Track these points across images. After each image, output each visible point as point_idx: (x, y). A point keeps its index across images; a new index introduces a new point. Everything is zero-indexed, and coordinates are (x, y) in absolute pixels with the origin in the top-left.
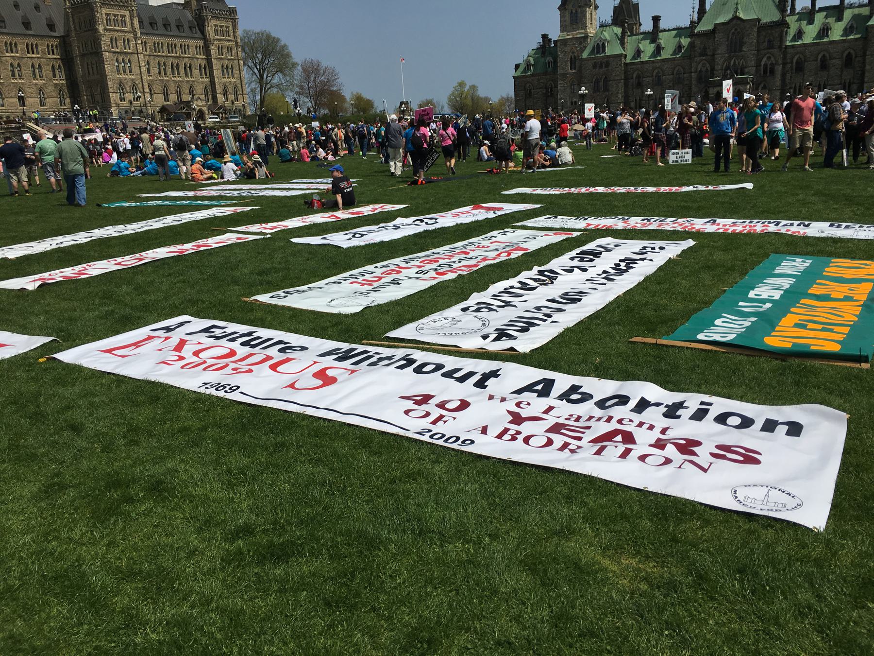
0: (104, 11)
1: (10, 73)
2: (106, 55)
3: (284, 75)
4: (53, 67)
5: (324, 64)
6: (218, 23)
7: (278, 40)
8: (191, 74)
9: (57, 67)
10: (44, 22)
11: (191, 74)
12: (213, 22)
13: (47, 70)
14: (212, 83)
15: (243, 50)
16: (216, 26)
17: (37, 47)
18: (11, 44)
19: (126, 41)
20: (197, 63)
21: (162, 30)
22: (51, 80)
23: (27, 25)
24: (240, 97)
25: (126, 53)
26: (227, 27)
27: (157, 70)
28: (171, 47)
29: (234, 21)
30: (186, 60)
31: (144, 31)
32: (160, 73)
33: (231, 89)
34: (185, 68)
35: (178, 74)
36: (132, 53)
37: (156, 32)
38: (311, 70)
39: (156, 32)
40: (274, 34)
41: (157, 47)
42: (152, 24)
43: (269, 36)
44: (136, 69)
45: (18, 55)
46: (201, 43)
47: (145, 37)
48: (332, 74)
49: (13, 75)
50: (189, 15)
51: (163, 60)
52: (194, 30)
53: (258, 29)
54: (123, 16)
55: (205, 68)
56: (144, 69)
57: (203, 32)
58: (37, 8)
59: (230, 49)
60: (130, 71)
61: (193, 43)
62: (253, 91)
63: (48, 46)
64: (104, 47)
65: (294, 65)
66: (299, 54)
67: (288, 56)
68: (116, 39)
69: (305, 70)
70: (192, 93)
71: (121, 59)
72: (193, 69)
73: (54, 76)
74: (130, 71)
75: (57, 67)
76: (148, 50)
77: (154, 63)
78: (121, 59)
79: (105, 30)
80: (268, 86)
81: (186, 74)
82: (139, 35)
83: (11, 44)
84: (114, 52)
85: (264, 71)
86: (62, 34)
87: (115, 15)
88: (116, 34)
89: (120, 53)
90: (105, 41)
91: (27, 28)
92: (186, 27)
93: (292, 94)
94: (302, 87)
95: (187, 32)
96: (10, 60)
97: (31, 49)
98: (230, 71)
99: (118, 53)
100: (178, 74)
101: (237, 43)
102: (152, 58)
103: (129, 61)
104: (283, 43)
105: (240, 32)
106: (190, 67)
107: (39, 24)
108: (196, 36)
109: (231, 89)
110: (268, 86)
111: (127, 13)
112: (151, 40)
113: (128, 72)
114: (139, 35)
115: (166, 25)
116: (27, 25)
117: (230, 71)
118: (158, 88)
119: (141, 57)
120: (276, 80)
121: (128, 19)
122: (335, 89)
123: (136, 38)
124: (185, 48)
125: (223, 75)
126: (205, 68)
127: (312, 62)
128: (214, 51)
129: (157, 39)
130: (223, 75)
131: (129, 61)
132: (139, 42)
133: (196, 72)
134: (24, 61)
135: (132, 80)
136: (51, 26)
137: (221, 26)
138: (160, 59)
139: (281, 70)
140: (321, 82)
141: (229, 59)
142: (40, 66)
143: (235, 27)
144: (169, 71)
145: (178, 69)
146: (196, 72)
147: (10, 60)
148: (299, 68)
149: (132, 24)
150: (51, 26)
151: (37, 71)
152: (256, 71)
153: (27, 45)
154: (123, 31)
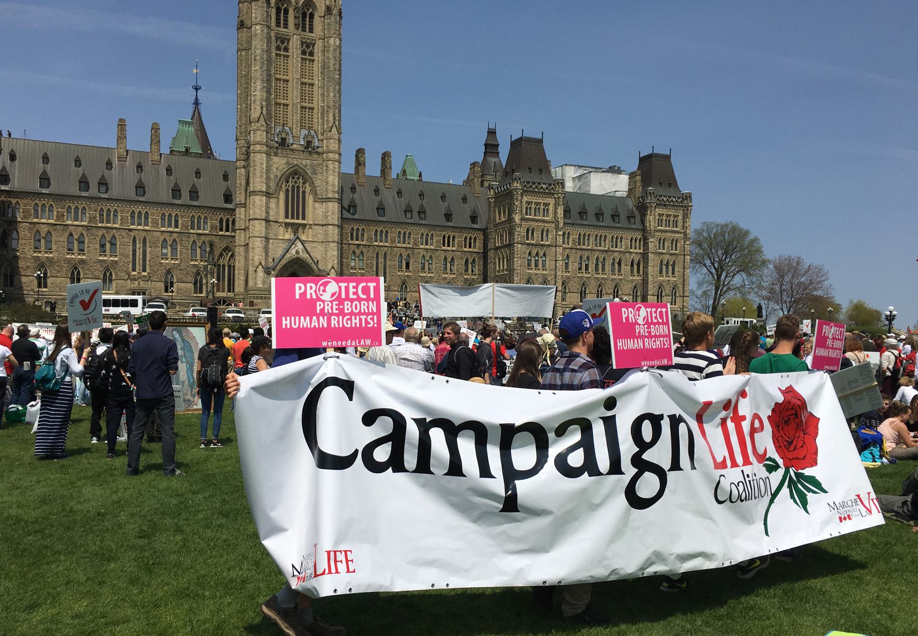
0: (525, 199)
1: (420, 266)
2: (518, 247)
3: (749, 274)
4: (467, 260)
5: (807, 261)
6: (665, 211)
7: (747, 232)
8: (619, 270)
9: (470, 261)
10: (468, 213)
11: (619, 270)
12: (659, 211)
13: (459, 264)
14: (645, 282)
15: (699, 244)
16: (660, 215)
17: (453, 240)
18: (427, 235)
19: (544, 233)
20: (628, 258)
21: (592, 220)
22: (461, 274)
23: (448, 217)
24: (679, 300)
26: (675, 216)
27: (577, 265)
28: (599, 239)
29: (686, 210)
30: (616, 254)
31: (568, 221)
32: (580, 269)
33: (667, 290)
34: (613, 264)
35: (603, 269)
36: (549, 246)
37: (585, 222)
38: (787, 269)
39: (585, 222)
40: (743, 226)
41: (581, 239)
42: (583, 213)
43: (735, 229)
44: (549, 264)
45: (432, 247)
46: (639, 235)
47: (568, 229)
48: (819, 274)
49: (423, 268)
50: (631, 204)
51: (586, 254)
52: (632, 220)
53: (722, 221)
54: (546, 205)
55: (638, 265)
57: (643, 222)
58: (464, 199)
59: (675, 242)
60: (544, 266)
61: (628, 235)
62: (705, 293)
63: (466, 238)
64: (517, 238)
65: (764, 263)
66: (773, 249)
67: (759, 251)
68: (533, 230)
69: (778, 269)
71: (534, 252)
72: (623, 265)
73: (466, 270)
74: (544, 266)
75: (470, 261)
76: (571, 242)
77: (574, 257)
78: (534, 252)
79: (522, 219)
80: (725, 289)
81: (613, 270)
82: (561, 225)
83: (427, 235)
84: (529, 244)
85: (722, 270)
86: (484, 227)
87: (537, 204)
88: (534, 224)
89: (536, 245)
90: (520, 233)
91: (448, 220)
92: (623, 216)
93: (757, 300)
94: (772, 291)
95: (624, 222)
96: (423, 252)
97: (446, 241)
98: (670, 268)
99: (533, 245)
100: (603, 269)
101: (685, 234)
103: (544, 255)
104: (751, 236)
105: (695, 223)
106: (619, 264)
107: (462, 218)
108: (634, 226)
109: (667, 290)
110: (725, 289)
111: (552, 201)
112: (575, 233)
113: (540, 266)
114: (561, 225)
115: (599, 215)
116: (448, 217)
117: (670, 268)
118: (574, 286)
120: (738, 280)
121: (551, 208)
122: (819, 293)
123: (557, 229)
124: (616, 241)
125: (661, 272)
126: (638, 265)
127: (789, 259)
128: (652, 244)
129: (582, 231)
130: (661, 272)
131: (544, 255)
132: (561, 233)
133: (626, 268)
134: (438, 253)
136: (474, 219)
137: (668, 216)
138: (584, 252)
139: (745, 268)
140: (800, 284)
141: (671, 254)
142: (453, 259)
143: (686, 216)
144: (592, 267)
145: (603, 266)
146: (626, 268)
147: (423, 252)
148: (771, 266)
149: (556, 213)
150: (474, 219)
151: (449, 264)
152: (714, 271)
153: (444, 237)
154: (544, 221)
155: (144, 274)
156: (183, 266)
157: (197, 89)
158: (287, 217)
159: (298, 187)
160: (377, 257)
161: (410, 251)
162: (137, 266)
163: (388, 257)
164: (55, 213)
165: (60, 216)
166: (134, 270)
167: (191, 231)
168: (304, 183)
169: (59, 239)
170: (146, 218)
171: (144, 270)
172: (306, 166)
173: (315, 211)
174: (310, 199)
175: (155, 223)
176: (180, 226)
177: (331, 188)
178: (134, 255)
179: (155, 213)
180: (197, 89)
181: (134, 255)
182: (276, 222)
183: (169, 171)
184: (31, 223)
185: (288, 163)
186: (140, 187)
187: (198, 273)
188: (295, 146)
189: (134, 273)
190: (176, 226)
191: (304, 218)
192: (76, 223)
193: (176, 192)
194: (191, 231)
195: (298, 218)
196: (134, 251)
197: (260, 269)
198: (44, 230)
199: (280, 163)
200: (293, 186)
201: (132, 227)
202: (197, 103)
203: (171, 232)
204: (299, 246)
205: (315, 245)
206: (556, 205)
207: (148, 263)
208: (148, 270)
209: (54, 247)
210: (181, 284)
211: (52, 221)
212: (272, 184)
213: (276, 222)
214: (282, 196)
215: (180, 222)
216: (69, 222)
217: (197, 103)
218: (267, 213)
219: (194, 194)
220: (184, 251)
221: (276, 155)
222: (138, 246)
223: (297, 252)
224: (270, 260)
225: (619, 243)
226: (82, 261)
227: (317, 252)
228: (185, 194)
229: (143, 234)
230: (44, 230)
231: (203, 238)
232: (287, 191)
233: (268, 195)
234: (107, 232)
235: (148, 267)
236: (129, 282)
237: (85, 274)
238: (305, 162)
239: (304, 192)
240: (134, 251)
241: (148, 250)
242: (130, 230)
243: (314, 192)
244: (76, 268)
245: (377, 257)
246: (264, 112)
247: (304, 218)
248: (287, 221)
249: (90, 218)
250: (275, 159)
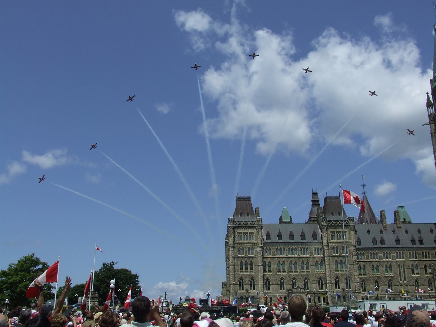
155: (401, 282)
156: (422, 277)
157: (363, 186)
162: (402, 279)
164: (365, 256)
165: (368, 258)
166: (401, 281)
167: (423, 259)
169: (369, 268)
170: (403, 255)
171: (405, 281)
175: (407, 257)
176: (418, 257)
178: (400, 273)
179: (406, 253)
180: (363, 186)
181: (400, 273)
183: (407, 232)
186: (398, 241)
187: (429, 280)
189: (401, 282)
190: (416, 258)
192: (374, 260)
193: (413, 241)
194: (423, 259)
196: (400, 271)
198: (362, 264)
201: (397, 260)
202: (364, 193)
207: (406, 276)
208: (407, 280)
209: (367, 272)
210: (422, 286)
211: (364, 260)
215: (417, 256)
216: (371, 260)
217: (364, 193)
219: (421, 242)
220: (422, 269)
222: (401, 269)
228: (417, 241)
229: (403, 263)
230: (362, 264)
231: (429, 262)
235: (407, 278)
236: (400, 286)
237: (381, 284)
240: (400, 271)
241: (406, 270)
242: (397, 261)
249: (380, 257)
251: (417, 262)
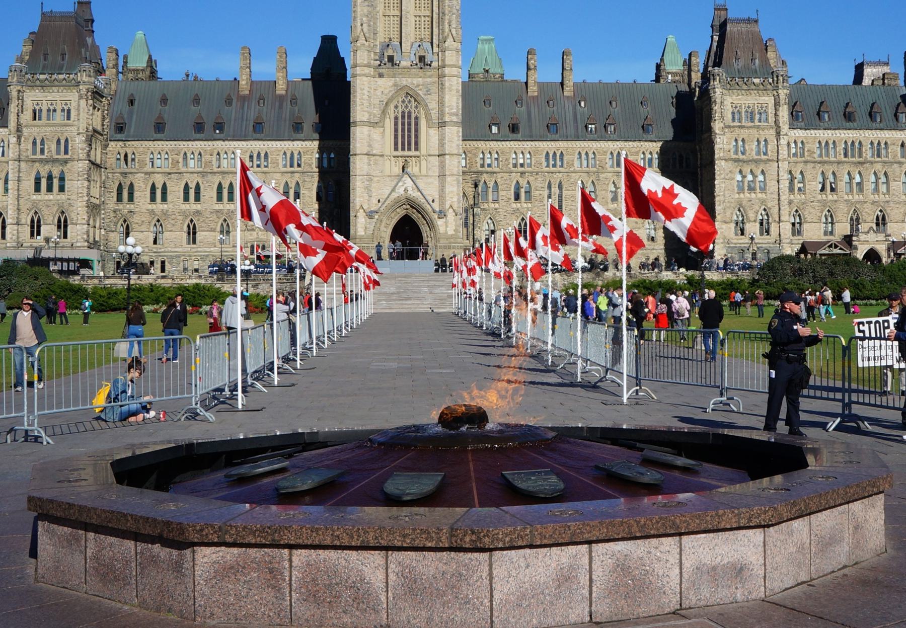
25: (756, 161)
32: (823, 189)
36: (768, 160)
44: (772, 185)
56: (785, 184)
70: (855, 222)
84: (737, 161)
102: (810, 166)
119: (784, 166)
121: (771, 110)
135: (763, 202)
158: (396, 149)
159: (410, 112)
160: (549, 187)
161: (593, 178)
163: (564, 186)
168: (416, 107)
172: (418, 86)
173: (429, 137)
174: (423, 123)
177: (447, 110)
182: (382, 156)
184: (146, 173)
185: (395, 85)
188: (403, 64)
191: (417, 149)
195: (409, 149)
197: (361, 214)
199: (386, 85)
200: (403, 112)
203: (293, 173)
204: (409, 183)
205: (430, 180)
206: (777, 104)
211: (168, 170)
212: (377, 111)
213: (382, 156)
214: (389, 124)
218: (370, 146)
221: (381, 76)
223: (406, 190)
224: (375, 201)
225: (883, 152)
226: (198, 213)
227: (430, 189)
232: (396, 118)
233: (373, 124)
234: (223, 178)
238: (417, 81)
239: (417, 118)
243: (428, 118)
244: (192, 221)
245: (549, 187)
246: (365, 30)
247: (417, 149)
248: (396, 153)
250: (381, 81)
251: (297, 175)
